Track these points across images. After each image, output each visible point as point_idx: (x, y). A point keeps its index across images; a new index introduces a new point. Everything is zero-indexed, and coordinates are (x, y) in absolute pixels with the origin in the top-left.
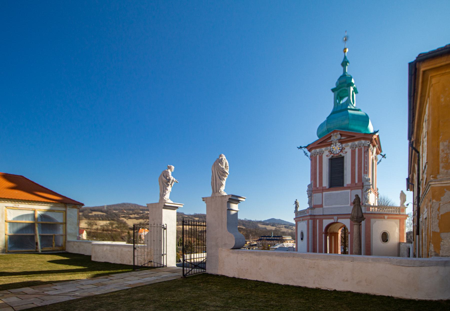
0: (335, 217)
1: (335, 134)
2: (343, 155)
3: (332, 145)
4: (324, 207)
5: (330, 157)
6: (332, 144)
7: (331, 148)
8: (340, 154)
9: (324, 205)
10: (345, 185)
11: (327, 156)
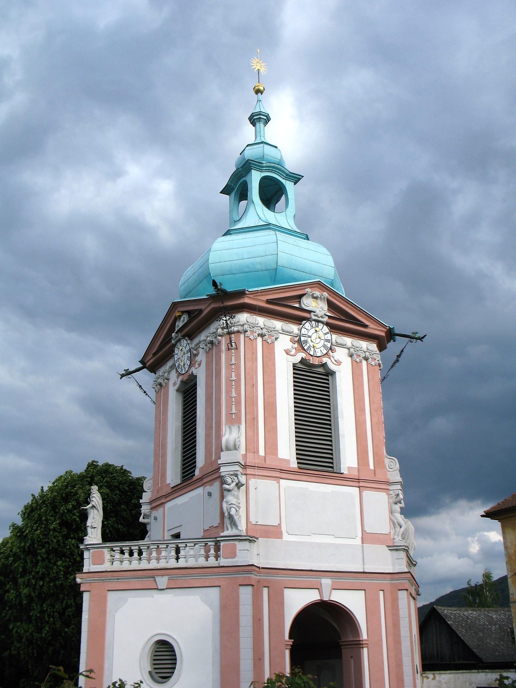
0: (327, 582)
1: (317, 293)
2: (332, 366)
3: (307, 325)
4: (286, 537)
5: (297, 359)
6: (308, 319)
7: (304, 331)
8: (325, 360)
9: (284, 528)
10: (344, 470)
11: (287, 352)
